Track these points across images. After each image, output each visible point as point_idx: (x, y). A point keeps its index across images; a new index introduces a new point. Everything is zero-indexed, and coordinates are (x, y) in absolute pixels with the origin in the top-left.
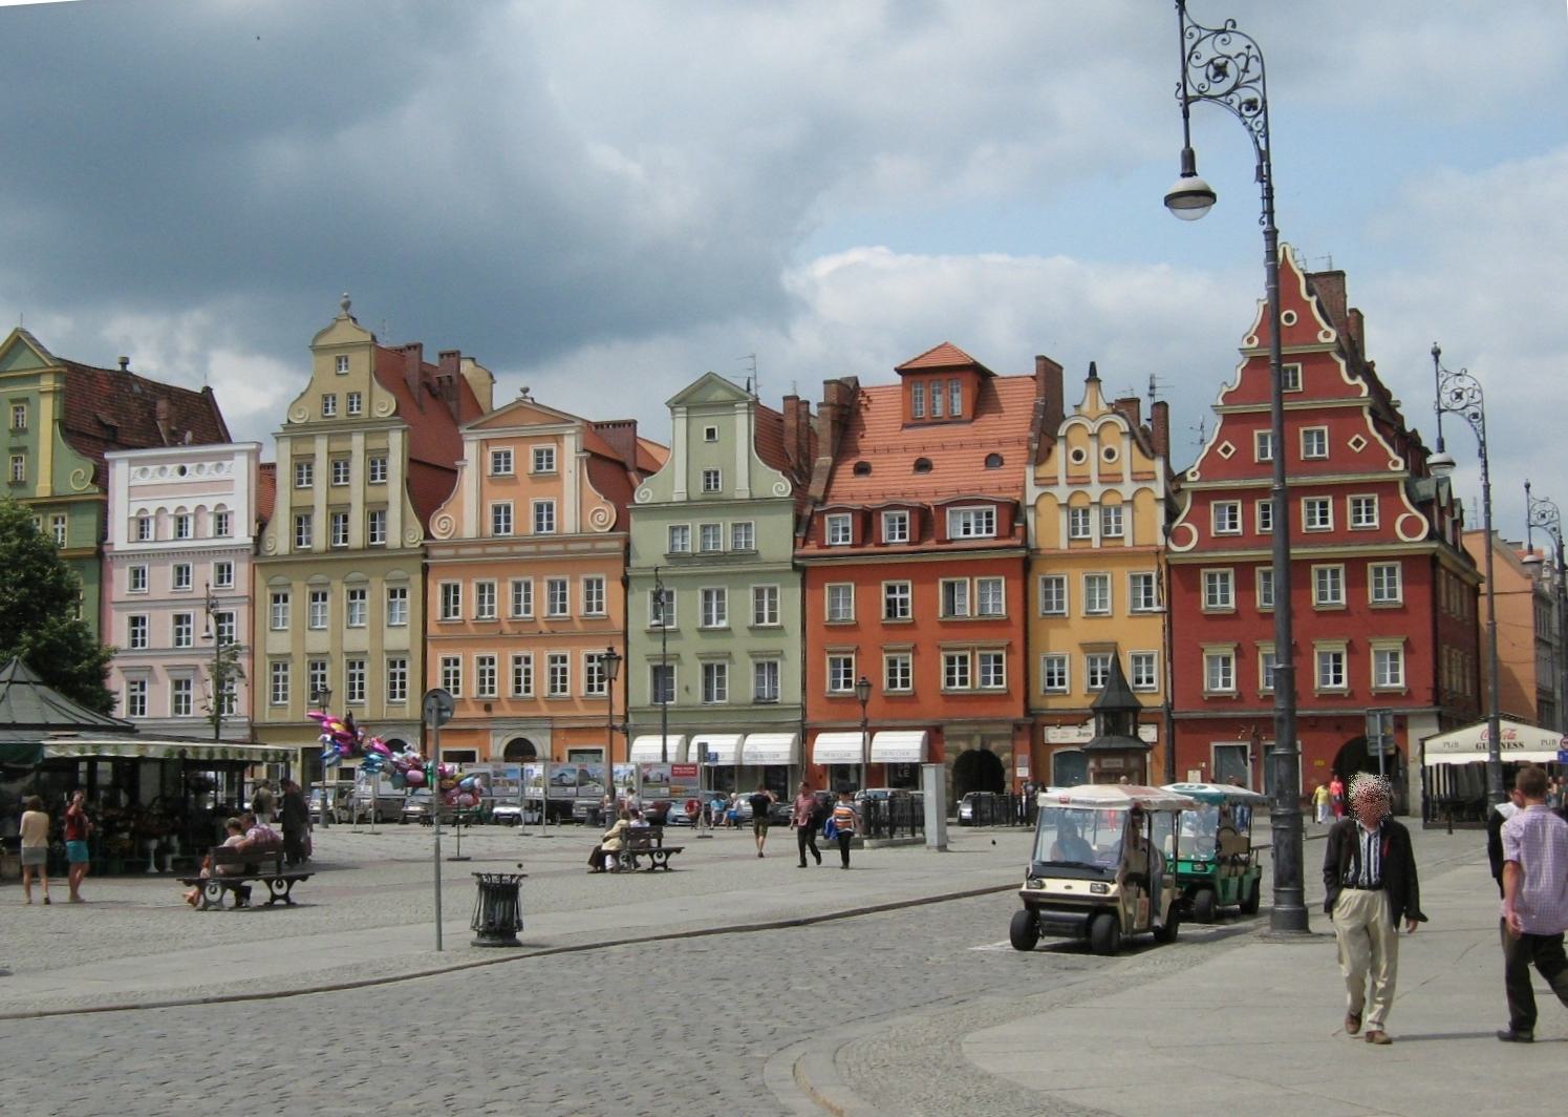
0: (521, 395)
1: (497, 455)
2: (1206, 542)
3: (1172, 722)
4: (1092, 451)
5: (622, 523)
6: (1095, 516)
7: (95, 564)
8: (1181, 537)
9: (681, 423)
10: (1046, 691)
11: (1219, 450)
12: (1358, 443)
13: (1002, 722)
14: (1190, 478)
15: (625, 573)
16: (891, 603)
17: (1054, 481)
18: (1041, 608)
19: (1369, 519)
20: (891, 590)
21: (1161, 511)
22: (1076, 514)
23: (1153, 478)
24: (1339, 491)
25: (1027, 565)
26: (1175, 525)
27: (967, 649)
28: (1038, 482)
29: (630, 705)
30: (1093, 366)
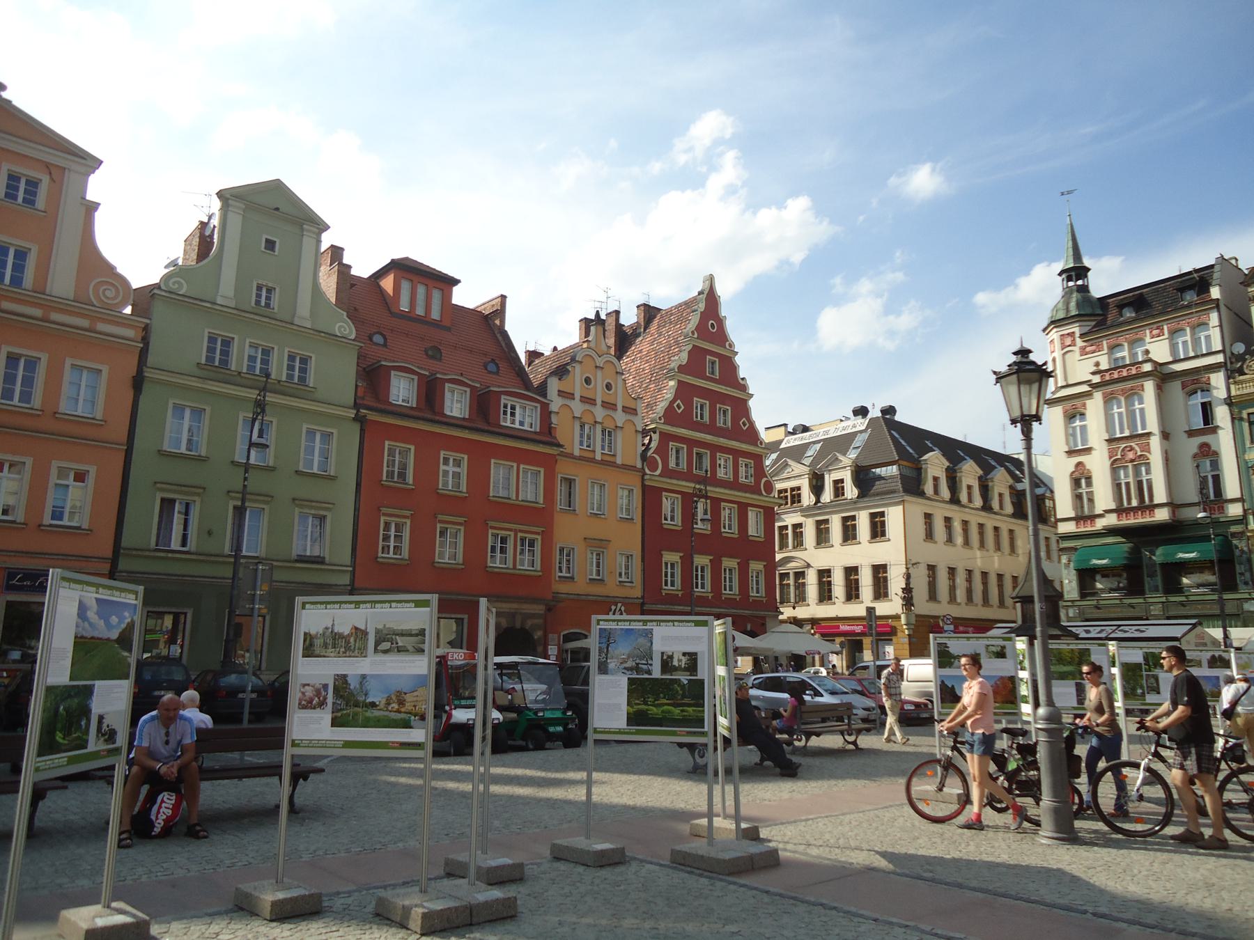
2: (667, 473)
8: (653, 467)
10: (559, 577)
11: (675, 405)
12: (745, 425)
13: (534, 600)
18: (559, 507)
24: (737, 454)
28: (561, 394)
29: (124, 544)
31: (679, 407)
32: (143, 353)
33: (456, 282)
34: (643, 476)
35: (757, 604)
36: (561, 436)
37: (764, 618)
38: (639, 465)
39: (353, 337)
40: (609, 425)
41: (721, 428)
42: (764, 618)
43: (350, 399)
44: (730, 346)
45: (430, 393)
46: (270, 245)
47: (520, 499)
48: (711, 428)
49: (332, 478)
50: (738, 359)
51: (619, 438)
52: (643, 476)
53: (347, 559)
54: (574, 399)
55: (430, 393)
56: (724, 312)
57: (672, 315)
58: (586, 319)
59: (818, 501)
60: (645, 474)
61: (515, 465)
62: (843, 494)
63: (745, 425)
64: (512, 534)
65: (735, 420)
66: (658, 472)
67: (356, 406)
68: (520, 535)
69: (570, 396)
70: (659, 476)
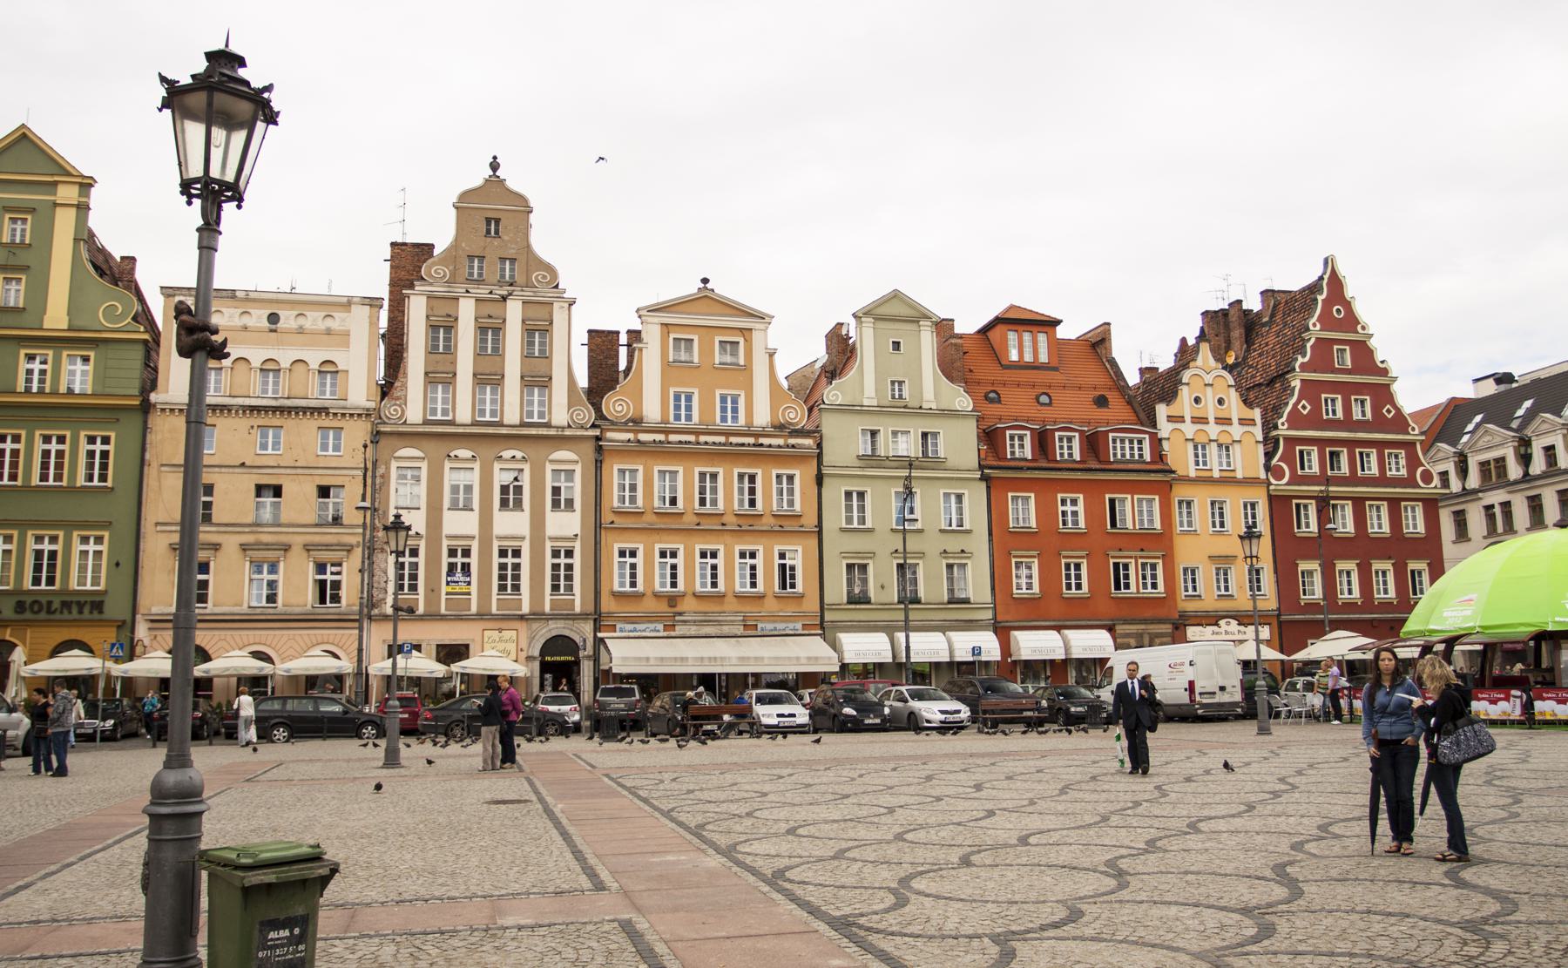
0: (702, 285)
2: (1295, 480)
3: (1280, 624)
4: (1210, 398)
7: (136, 419)
8: (1279, 474)
11: (1299, 407)
12: (1389, 411)
13: (1160, 621)
14: (1280, 427)
15: (819, 470)
18: (1179, 529)
19: (1398, 470)
21: (1261, 449)
22: (1199, 447)
23: (1252, 422)
24: (1380, 445)
26: (1274, 461)
27: (1131, 557)
29: (827, 601)
31: (1304, 407)
32: (820, 456)
33: (1058, 322)
34: (1268, 487)
35: (1386, 606)
36: (1172, 462)
38: (1263, 475)
39: (970, 408)
40: (1224, 440)
41: (1358, 421)
43: (972, 460)
44: (1363, 328)
45: (1043, 441)
46: (897, 345)
47: (1137, 527)
49: (968, 532)
50: (1373, 343)
51: (1236, 450)
52: (1268, 487)
53: (989, 599)
54: (1184, 422)
55: (1043, 441)
56: (1349, 293)
57: (1296, 301)
58: (1207, 312)
59: (1526, 474)
60: (1269, 484)
61: (1129, 496)
62: (1556, 465)
63: (1389, 411)
64: (1133, 561)
65: (1376, 409)
66: (1285, 480)
67: (981, 467)
68: (1140, 561)
69: (1181, 419)
70: (1286, 484)
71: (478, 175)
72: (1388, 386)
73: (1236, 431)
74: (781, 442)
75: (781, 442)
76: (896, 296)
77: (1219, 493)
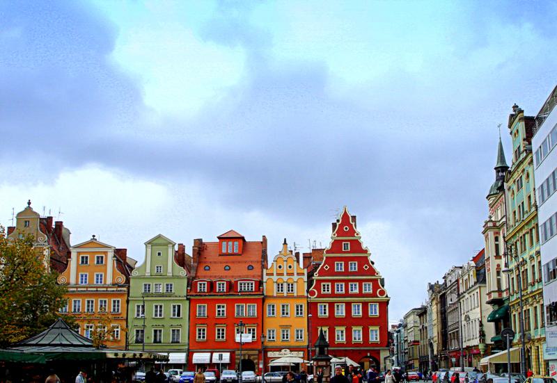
1: (83, 258)
5: (128, 281)
6: (285, 286)
8: (312, 294)
9: (149, 250)
12: (366, 267)
16: (219, 311)
17: (272, 274)
18: (267, 315)
19: (369, 290)
20: (219, 307)
21: (306, 284)
23: (303, 274)
24: (360, 281)
25: (263, 300)
26: (311, 289)
30: (285, 240)
37: (379, 350)
38: (306, 294)
42: (379, 350)
45: (212, 286)
46: (159, 254)
48: (346, 273)
50: (361, 240)
53: (187, 341)
55: (212, 286)
60: (307, 297)
63: (366, 267)
65: (360, 266)
66: (315, 296)
71: (21, 207)
72: (367, 257)
73: (295, 278)
74: (115, 289)
75: (115, 289)
76: (159, 237)
77: (285, 302)
